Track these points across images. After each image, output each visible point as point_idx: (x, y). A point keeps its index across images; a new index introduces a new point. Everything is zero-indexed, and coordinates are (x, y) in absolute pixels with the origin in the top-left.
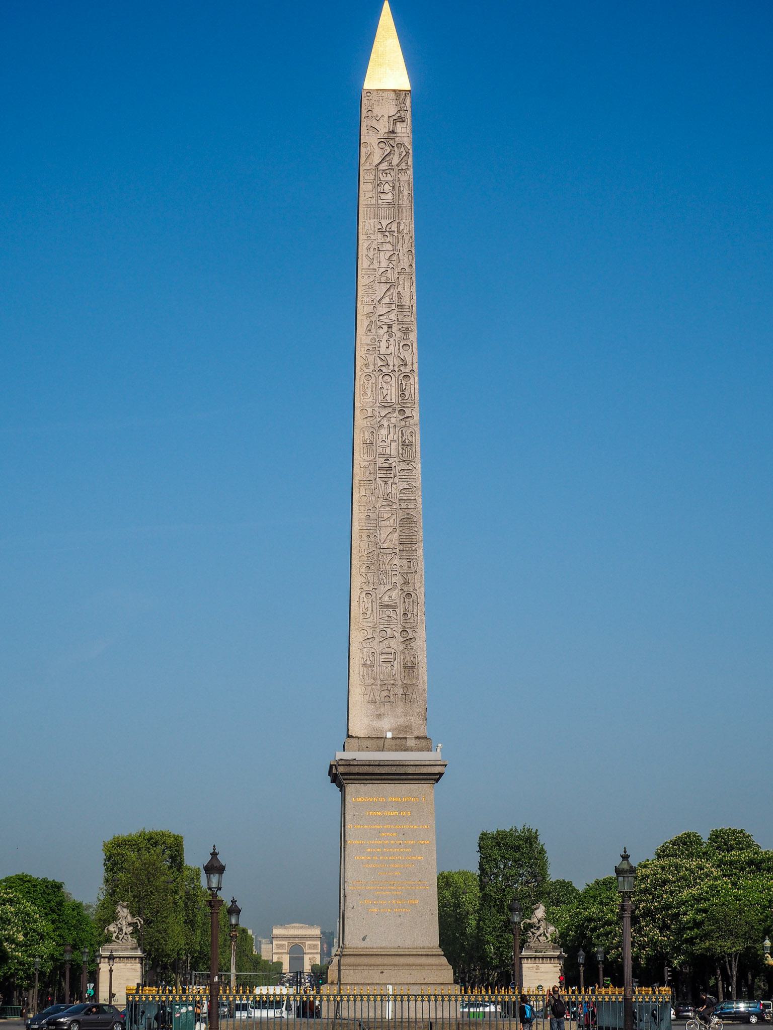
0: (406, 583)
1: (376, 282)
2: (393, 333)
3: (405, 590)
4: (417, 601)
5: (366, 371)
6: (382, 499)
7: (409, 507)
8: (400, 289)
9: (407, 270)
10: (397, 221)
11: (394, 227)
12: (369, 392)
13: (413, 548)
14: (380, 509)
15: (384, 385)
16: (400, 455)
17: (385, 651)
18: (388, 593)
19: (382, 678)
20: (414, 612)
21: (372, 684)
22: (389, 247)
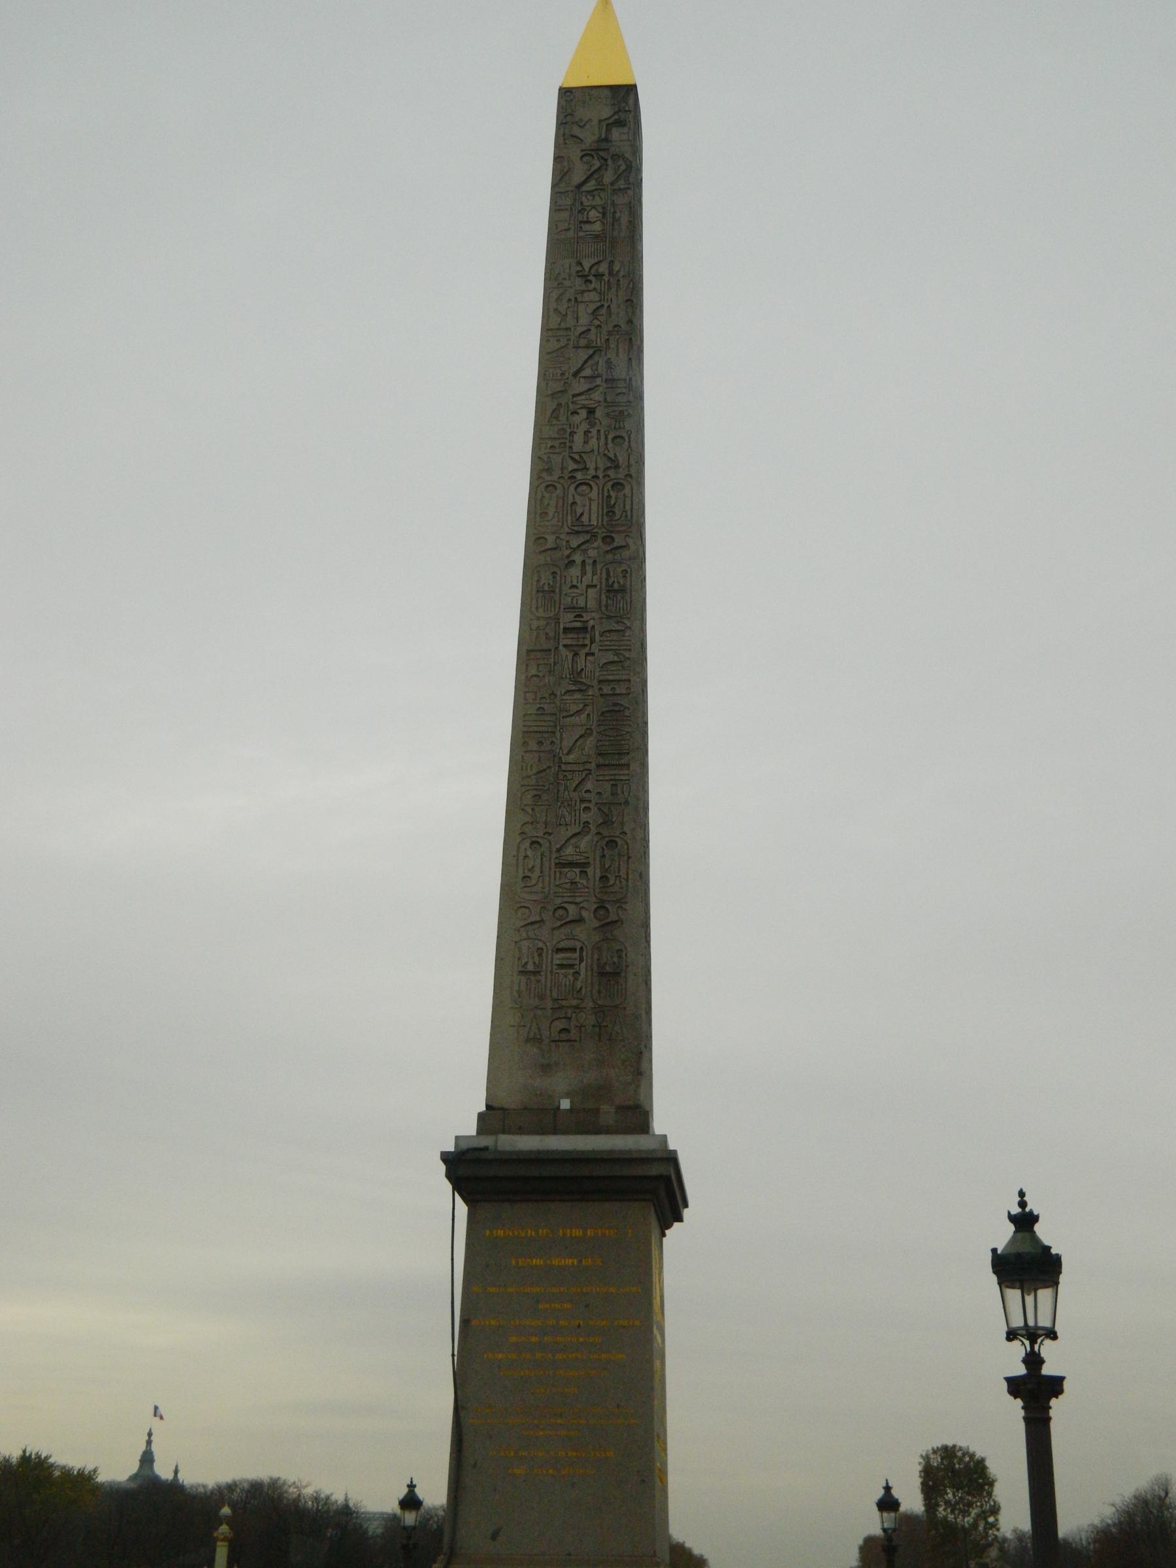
0: (608, 822)
1: (570, 347)
2: (597, 421)
3: (605, 832)
4: (628, 854)
5: (549, 478)
6: (568, 680)
7: (618, 691)
8: (611, 355)
9: (624, 326)
10: (610, 259)
11: (603, 268)
12: (551, 513)
13: (623, 762)
14: (564, 697)
15: (578, 499)
16: (603, 609)
17: (563, 945)
18: (573, 841)
19: (555, 995)
20: (621, 874)
21: (536, 1007)
22: (593, 296)
